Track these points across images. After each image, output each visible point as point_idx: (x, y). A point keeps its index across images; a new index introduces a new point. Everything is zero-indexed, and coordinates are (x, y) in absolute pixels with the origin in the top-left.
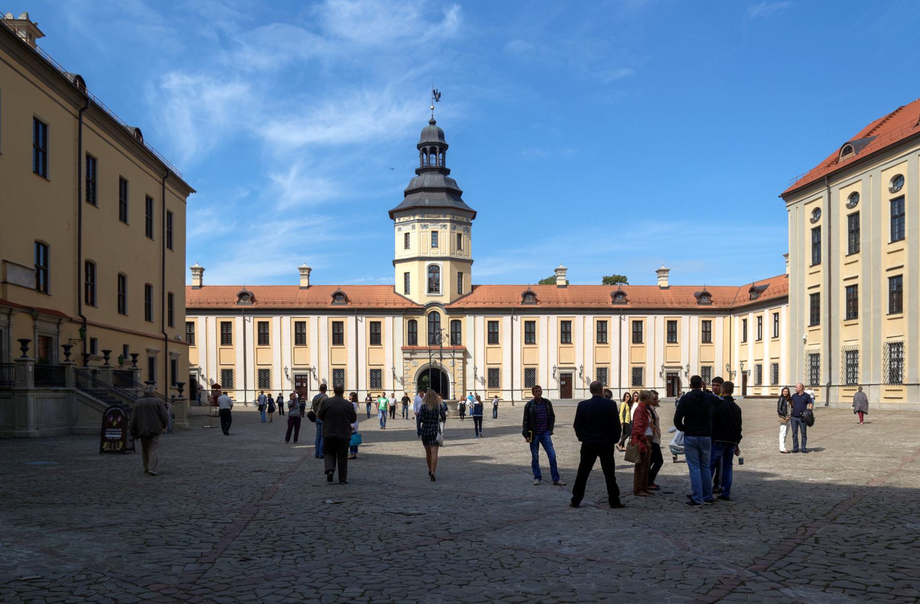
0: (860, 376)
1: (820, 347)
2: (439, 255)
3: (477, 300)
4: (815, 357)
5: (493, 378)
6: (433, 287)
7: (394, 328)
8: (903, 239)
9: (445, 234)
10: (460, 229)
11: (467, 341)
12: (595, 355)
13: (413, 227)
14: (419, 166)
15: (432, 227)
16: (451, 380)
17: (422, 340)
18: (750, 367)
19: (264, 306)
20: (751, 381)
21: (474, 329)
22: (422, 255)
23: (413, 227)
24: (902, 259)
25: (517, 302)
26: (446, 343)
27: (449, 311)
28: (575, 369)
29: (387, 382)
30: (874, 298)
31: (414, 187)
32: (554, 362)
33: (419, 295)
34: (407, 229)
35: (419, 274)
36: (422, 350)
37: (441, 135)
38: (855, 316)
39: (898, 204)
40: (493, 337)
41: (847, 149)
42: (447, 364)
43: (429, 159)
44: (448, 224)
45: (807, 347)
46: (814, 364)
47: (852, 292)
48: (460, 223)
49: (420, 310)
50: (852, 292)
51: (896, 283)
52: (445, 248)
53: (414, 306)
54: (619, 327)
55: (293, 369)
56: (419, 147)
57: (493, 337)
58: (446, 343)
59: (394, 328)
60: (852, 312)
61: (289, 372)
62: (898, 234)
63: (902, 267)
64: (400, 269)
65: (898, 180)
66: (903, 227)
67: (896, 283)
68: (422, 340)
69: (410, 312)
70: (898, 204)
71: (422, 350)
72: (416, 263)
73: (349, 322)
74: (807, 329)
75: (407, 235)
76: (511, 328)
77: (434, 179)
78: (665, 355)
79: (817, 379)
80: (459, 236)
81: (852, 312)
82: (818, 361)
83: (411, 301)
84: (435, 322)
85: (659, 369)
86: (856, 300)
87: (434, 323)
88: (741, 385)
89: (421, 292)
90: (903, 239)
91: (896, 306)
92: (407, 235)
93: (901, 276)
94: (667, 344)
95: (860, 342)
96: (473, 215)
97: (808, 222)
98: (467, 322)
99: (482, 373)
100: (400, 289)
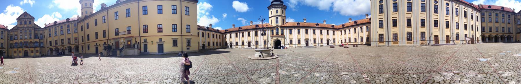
3: (287, 25)
5: (291, 41)
7: (269, 33)
9: (280, 10)
11: (285, 34)
15: (276, 9)
17: (275, 34)
21: (286, 32)
25: (296, 25)
27: (281, 27)
32: (304, 38)
33: (274, 24)
34: (271, 10)
35: (274, 19)
36: (275, 36)
40: (291, 33)
49: (274, 27)
52: (280, 13)
54: (318, 31)
57: (291, 33)
59: (269, 33)
64: (270, 19)
68: (275, 34)
69: (272, 28)
71: (275, 36)
76: (295, 31)
98: (285, 31)
99: (289, 42)
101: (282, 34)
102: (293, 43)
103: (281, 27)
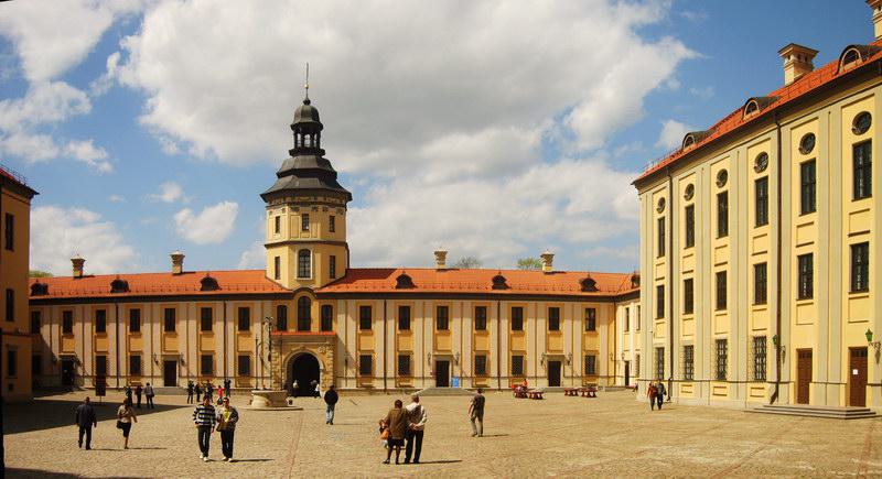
0: (695, 371)
1: (665, 343)
2: (309, 239)
4: (660, 350)
6: (303, 272)
8: (815, 211)
10: (332, 211)
12: (474, 343)
13: (284, 210)
14: (293, 147)
16: (321, 367)
18: (631, 357)
19: (136, 294)
20: (632, 373)
22: (292, 239)
23: (284, 210)
24: (868, 222)
26: (315, 327)
28: (452, 356)
29: (256, 369)
30: (833, 272)
31: (285, 169)
33: (287, 281)
34: (277, 212)
37: (314, 114)
38: (810, 294)
39: (862, 151)
41: (751, 106)
42: (317, 352)
43: (303, 139)
44: (320, 207)
45: (656, 341)
46: (721, 353)
47: (806, 262)
48: (333, 205)
49: (288, 296)
50: (806, 262)
51: (860, 253)
53: (284, 291)
55: (162, 356)
56: (293, 127)
58: (315, 327)
60: (806, 291)
61: (159, 359)
62: (862, 189)
63: (868, 232)
65: (862, 122)
66: (870, 180)
67: (860, 253)
70: (862, 151)
72: (286, 248)
73: (218, 307)
74: (846, 296)
75: (278, 218)
77: (307, 162)
78: (547, 344)
79: (691, 374)
80: (332, 218)
81: (806, 291)
82: (725, 349)
83: (280, 286)
84: (304, 307)
85: (540, 358)
86: (725, 290)
87: (304, 308)
88: (624, 375)
89: (290, 277)
90: (815, 211)
91: (859, 281)
92: (278, 218)
93: (867, 244)
94: (549, 332)
95: (694, 338)
96: (349, 197)
97: (714, 185)
100: (271, 274)
101: (326, 324)
102: (378, 370)
103: (320, 296)
